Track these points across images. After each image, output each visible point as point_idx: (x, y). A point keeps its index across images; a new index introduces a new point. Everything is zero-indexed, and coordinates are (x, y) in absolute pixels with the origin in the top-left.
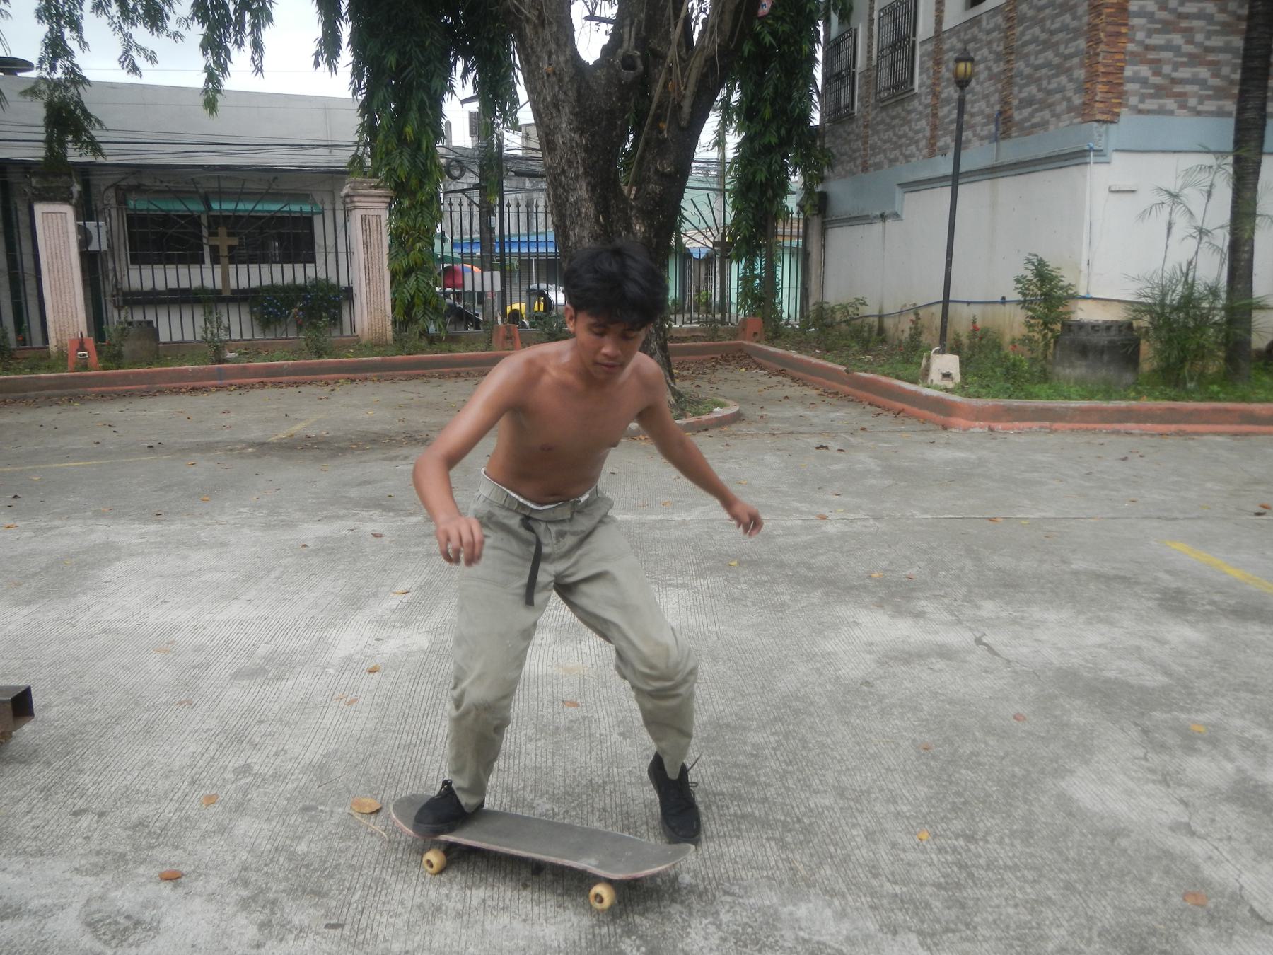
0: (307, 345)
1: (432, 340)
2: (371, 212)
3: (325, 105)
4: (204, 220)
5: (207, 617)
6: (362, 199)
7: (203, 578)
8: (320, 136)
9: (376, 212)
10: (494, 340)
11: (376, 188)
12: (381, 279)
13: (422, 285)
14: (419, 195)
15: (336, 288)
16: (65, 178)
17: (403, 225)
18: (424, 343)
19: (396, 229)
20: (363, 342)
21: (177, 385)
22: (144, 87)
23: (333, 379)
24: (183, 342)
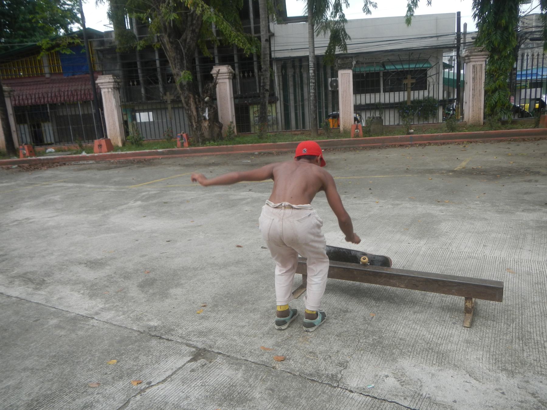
0: (447, 126)
1: (504, 123)
2: (478, 63)
3: (437, 18)
4: (381, 74)
5: (516, 257)
6: (474, 57)
7: (493, 235)
8: (433, 33)
9: (480, 63)
10: (541, 122)
11: (481, 51)
12: (480, 95)
13: (502, 96)
14: (504, 53)
15: (434, 100)
16: (350, 59)
17: (493, 68)
18: (500, 124)
19: (490, 70)
20: (469, 124)
21: (392, 144)
22: (362, 20)
23: (461, 142)
24: (389, 126)
